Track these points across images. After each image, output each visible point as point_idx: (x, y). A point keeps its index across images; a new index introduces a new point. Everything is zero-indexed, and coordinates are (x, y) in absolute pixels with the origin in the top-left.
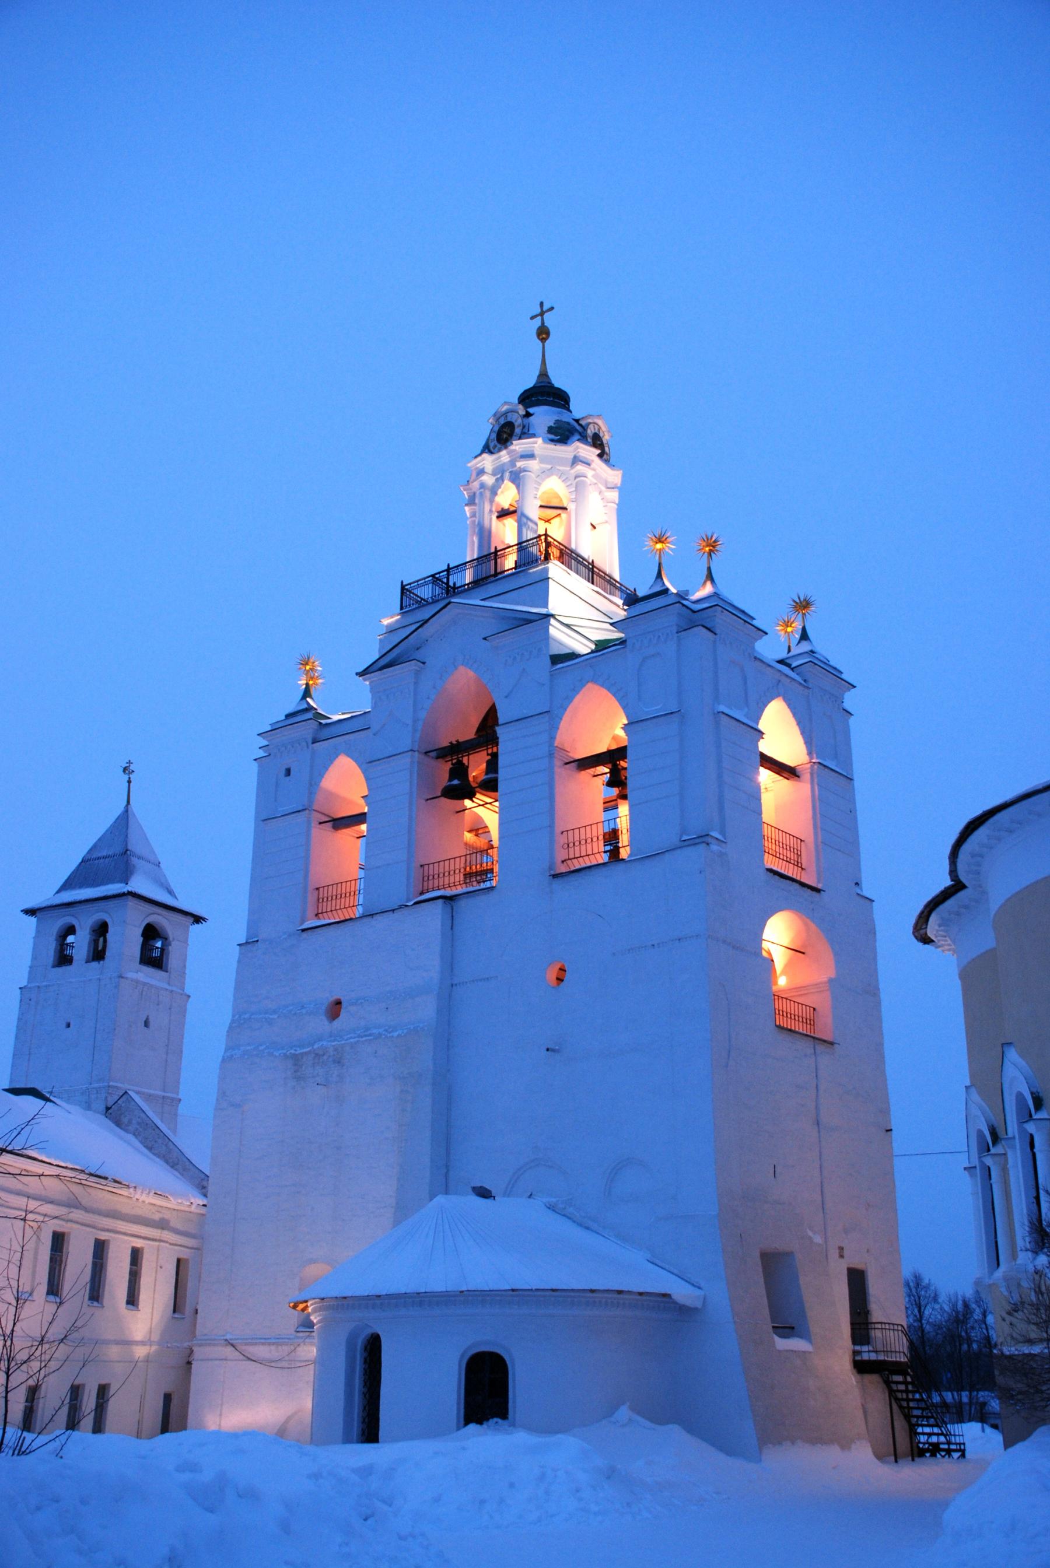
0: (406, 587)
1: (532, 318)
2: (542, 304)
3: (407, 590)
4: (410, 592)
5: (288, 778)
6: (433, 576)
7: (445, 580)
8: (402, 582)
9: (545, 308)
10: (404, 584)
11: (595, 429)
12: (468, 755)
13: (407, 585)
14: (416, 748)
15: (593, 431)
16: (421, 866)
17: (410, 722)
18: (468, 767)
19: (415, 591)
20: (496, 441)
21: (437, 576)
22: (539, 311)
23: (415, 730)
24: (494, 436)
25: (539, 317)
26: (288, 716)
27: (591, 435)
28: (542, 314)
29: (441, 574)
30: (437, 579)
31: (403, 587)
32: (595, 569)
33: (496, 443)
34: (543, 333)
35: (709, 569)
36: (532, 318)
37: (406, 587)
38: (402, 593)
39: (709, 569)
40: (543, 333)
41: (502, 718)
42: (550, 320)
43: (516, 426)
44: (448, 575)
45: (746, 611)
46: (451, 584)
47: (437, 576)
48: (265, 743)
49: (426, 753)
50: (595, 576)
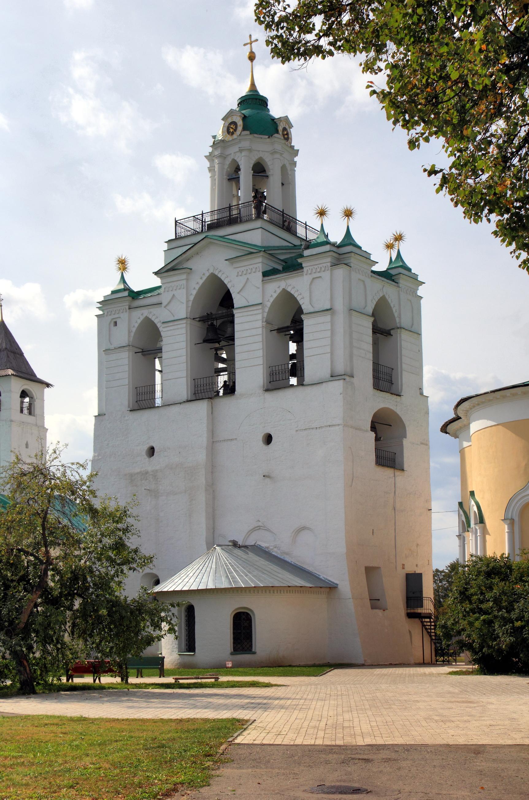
1: (245, 45)
5: (116, 327)
6: (194, 217)
9: (253, 39)
12: (217, 320)
14: (188, 317)
17: (185, 301)
20: (226, 133)
21: (196, 217)
23: (187, 307)
25: (249, 45)
26: (113, 292)
28: (251, 44)
30: (197, 218)
31: (176, 222)
32: (284, 215)
36: (245, 45)
38: (176, 225)
41: (236, 303)
44: (202, 216)
46: (204, 221)
49: (194, 319)
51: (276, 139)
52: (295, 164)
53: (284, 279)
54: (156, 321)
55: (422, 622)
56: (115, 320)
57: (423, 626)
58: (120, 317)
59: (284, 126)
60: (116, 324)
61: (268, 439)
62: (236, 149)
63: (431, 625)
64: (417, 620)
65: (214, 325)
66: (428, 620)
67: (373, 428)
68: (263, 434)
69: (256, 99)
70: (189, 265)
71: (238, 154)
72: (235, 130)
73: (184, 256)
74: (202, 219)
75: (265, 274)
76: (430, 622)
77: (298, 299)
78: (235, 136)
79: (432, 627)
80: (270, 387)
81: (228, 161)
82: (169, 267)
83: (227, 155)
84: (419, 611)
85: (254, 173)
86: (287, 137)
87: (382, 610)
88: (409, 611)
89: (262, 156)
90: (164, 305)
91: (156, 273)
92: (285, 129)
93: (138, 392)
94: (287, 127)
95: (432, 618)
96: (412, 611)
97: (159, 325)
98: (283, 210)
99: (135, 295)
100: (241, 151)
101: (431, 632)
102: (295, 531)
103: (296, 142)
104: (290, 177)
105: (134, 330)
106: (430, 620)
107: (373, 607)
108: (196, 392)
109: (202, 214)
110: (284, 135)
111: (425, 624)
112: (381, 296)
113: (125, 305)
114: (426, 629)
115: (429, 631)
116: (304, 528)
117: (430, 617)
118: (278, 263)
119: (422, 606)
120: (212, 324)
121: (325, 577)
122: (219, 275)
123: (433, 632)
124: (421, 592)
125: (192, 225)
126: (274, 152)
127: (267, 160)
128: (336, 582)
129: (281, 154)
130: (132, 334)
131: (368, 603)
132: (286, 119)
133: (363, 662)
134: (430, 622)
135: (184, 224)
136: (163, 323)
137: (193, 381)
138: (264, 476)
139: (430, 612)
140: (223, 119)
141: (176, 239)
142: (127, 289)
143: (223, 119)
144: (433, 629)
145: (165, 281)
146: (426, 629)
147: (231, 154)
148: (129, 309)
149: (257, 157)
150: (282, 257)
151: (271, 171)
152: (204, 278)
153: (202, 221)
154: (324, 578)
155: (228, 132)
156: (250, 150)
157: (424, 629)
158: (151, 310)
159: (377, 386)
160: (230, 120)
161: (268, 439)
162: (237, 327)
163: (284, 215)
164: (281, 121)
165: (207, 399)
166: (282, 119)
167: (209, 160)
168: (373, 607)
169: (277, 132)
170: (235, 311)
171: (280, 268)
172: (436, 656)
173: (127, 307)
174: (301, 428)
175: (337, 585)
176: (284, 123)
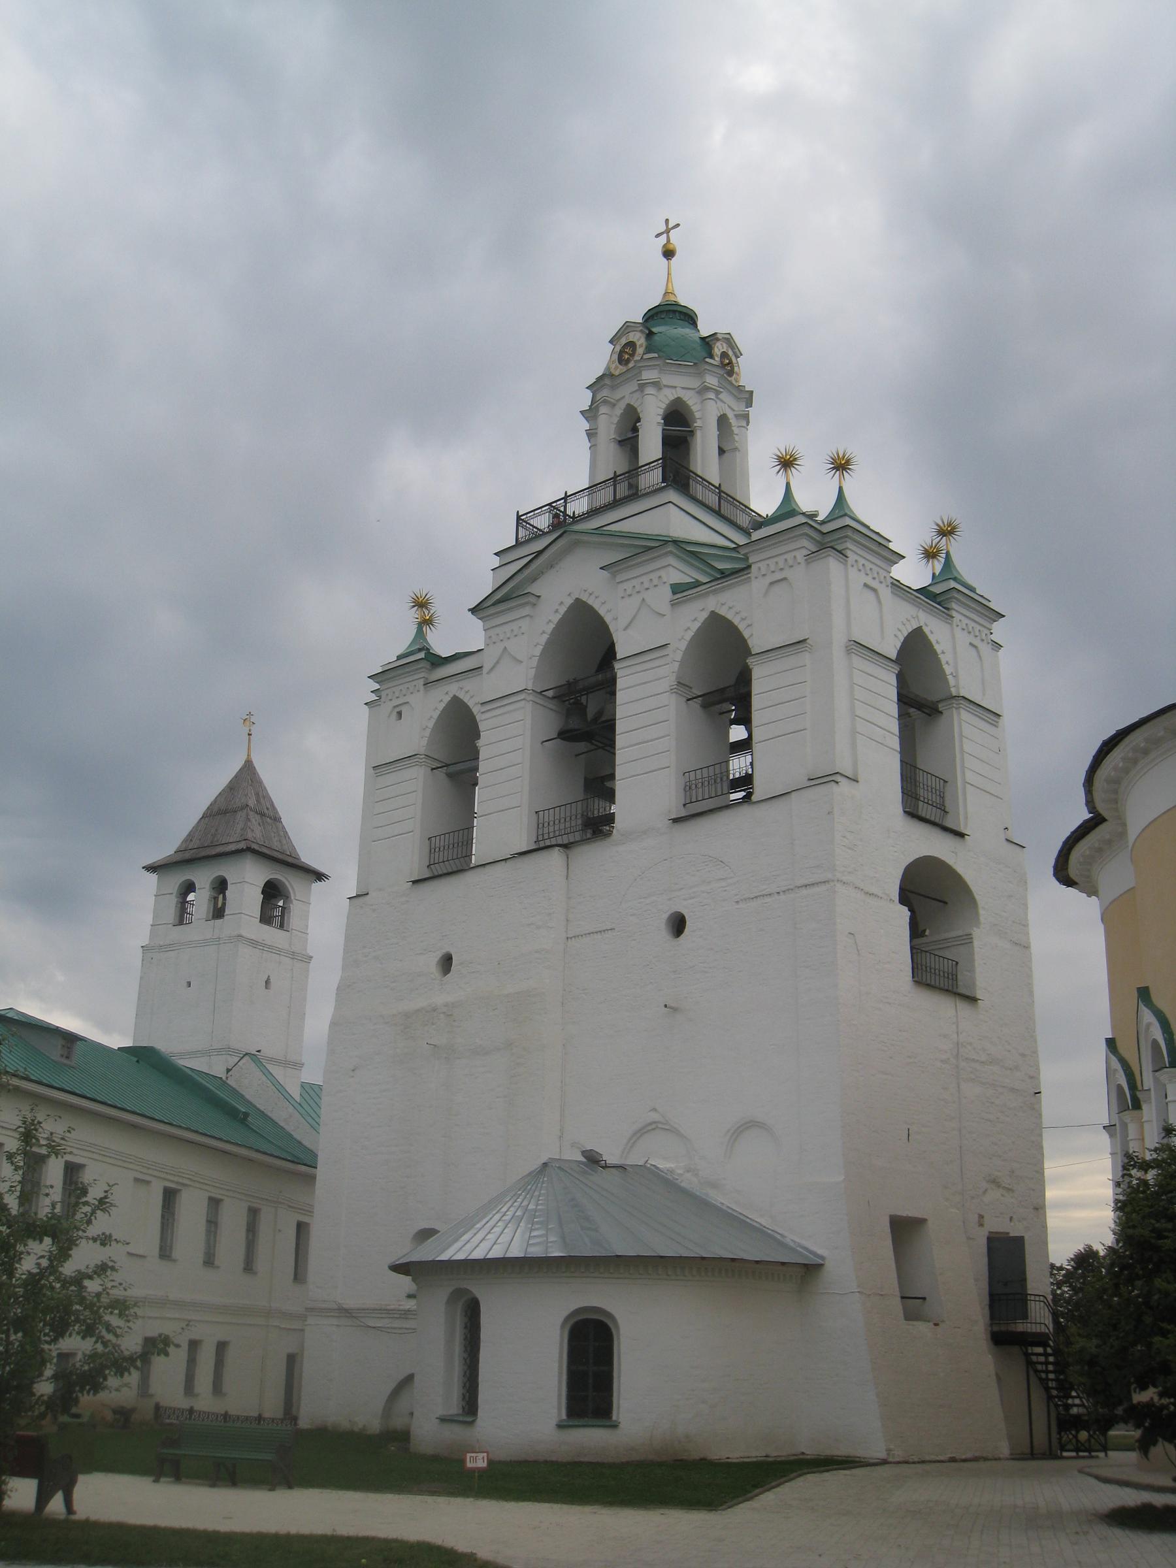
0: (522, 518)
1: (658, 236)
2: (667, 221)
6: (550, 504)
7: (562, 509)
8: (518, 512)
9: (670, 226)
11: (723, 348)
16: (536, 812)
18: (586, 707)
19: (531, 522)
21: (554, 505)
22: (663, 228)
24: (616, 357)
26: (399, 658)
27: (719, 353)
28: (667, 231)
29: (558, 503)
31: (519, 517)
33: (618, 364)
34: (669, 253)
35: (841, 489)
36: (658, 236)
37: (522, 518)
39: (841, 489)
40: (669, 253)
43: (638, 346)
44: (566, 502)
45: (881, 533)
47: (554, 505)
48: (377, 686)
50: (722, 501)
51: (707, 367)
52: (746, 417)
53: (715, 592)
54: (471, 704)
55: (1027, 1355)
56: (398, 709)
57: (1030, 1364)
58: (408, 703)
59: (725, 350)
61: (678, 925)
62: (633, 386)
63: (1047, 1363)
64: (1016, 1349)
65: (582, 704)
66: (1040, 1350)
68: (666, 916)
69: (674, 312)
70: (535, 588)
72: (633, 355)
73: (527, 572)
76: (1046, 1355)
77: (741, 627)
78: (631, 365)
79: (1051, 1368)
80: (683, 813)
81: (619, 411)
83: (618, 400)
84: (1020, 1327)
86: (728, 366)
87: (931, 1324)
88: (996, 1329)
89: (682, 397)
90: (485, 670)
91: (473, 611)
92: (724, 355)
94: (730, 353)
95: (1049, 1346)
96: (1003, 1328)
97: (475, 710)
98: (720, 484)
99: (436, 661)
101: (1048, 1379)
102: (732, 1132)
103: (747, 373)
104: (737, 438)
106: (1045, 1350)
107: (911, 1316)
108: (540, 838)
111: (1034, 1358)
114: (1036, 1371)
115: (1043, 1375)
116: (749, 1125)
117: (1044, 1345)
119: (1025, 1316)
120: (577, 703)
121: (797, 1240)
122: (590, 602)
123: (1052, 1380)
124: (1023, 1280)
126: (703, 390)
127: (690, 403)
128: (820, 1252)
129: (717, 393)
131: (896, 1304)
132: (729, 340)
133: (882, 1455)
134: (1046, 1355)
138: (666, 1006)
139: (1043, 1329)
140: (611, 342)
142: (426, 649)
143: (611, 342)
144: (1051, 1372)
145: (490, 624)
146: (1036, 1371)
147: (624, 397)
152: (563, 610)
154: (794, 1242)
155: (621, 360)
156: (657, 385)
157: (1031, 1373)
159: (912, 813)
160: (623, 341)
161: (678, 925)
162: (620, 697)
163: (722, 494)
164: (718, 340)
165: (558, 848)
167: (586, 419)
168: (911, 1316)
169: (711, 356)
170: (617, 666)
172: (1059, 1433)
173: (422, 682)
175: (822, 1258)
176: (725, 345)
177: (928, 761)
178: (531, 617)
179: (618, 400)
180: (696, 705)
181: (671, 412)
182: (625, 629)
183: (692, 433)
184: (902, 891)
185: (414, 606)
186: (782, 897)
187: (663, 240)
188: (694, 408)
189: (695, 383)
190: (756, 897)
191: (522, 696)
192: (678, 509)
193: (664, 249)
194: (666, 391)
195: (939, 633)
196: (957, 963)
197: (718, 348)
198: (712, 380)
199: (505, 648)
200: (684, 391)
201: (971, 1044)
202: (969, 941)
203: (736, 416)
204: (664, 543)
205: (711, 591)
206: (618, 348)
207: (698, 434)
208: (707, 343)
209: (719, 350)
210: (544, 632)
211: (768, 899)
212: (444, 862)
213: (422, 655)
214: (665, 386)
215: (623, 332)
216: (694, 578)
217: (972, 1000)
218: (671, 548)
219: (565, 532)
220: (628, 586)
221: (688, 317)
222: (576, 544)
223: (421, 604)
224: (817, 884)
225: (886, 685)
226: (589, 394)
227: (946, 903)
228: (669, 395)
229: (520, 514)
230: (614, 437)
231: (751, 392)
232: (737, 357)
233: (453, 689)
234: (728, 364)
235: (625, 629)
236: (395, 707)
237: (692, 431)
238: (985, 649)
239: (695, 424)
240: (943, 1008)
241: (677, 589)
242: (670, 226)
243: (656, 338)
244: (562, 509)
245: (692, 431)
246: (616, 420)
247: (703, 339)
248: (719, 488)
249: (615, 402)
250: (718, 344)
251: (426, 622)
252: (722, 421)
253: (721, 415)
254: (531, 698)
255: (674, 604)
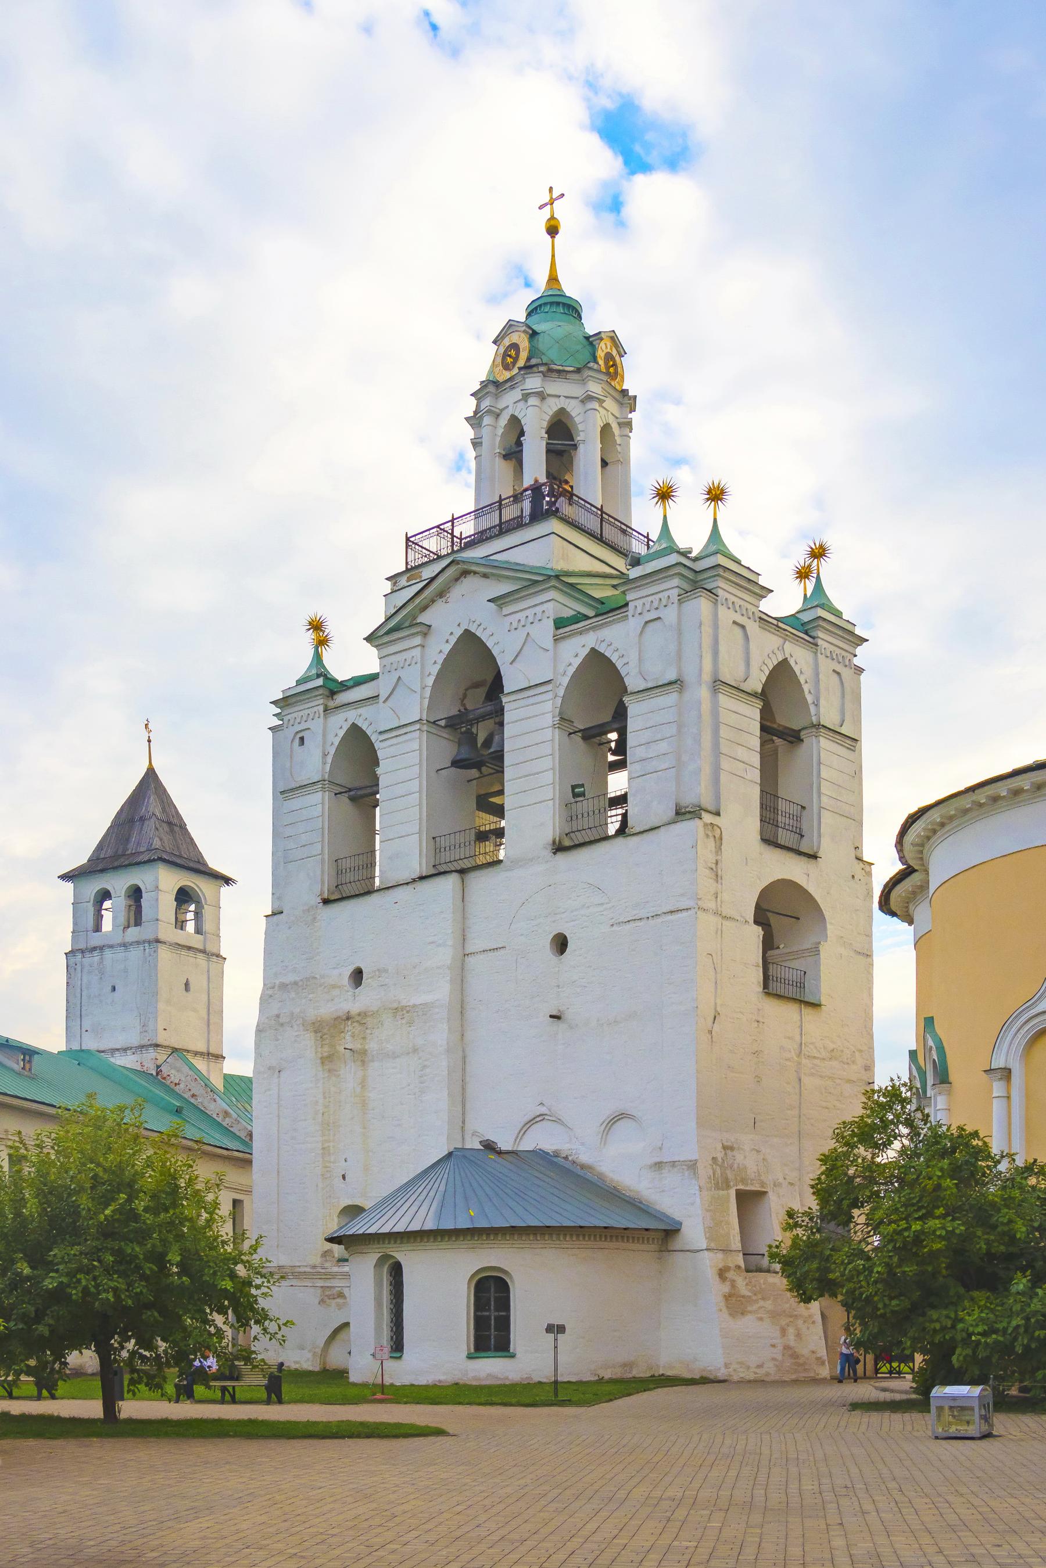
0: (412, 539)
1: (541, 207)
3: (413, 543)
4: (416, 544)
6: (438, 527)
7: (450, 531)
10: (408, 536)
11: (607, 347)
12: (477, 723)
13: (411, 537)
15: (605, 351)
17: (418, 689)
18: (477, 735)
21: (442, 527)
22: (547, 199)
23: (422, 698)
24: (499, 360)
28: (552, 204)
30: (443, 530)
31: (408, 539)
34: (553, 230)
36: (541, 207)
37: (412, 539)
38: (407, 546)
40: (553, 230)
42: (561, 210)
44: (453, 525)
46: (457, 533)
47: (442, 527)
50: (604, 523)
51: (591, 373)
54: (369, 732)
56: (300, 735)
58: (309, 729)
59: (609, 350)
60: (302, 739)
61: (561, 944)
62: (516, 394)
67: (761, 917)
69: (558, 304)
71: (521, 404)
74: (453, 530)
75: (560, 623)
81: (504, 421)
82: (392, 624)
83: (502, 410)
85: (549, 438)
86: (613, 370)
90: (382, 699)
91: (369, 639)
92: (609, 357)
93: (340, 867)
94: (614, 353)
97: (373, 738)
100: (526, 397)
105: (332, 751)
109: (453, 521)
110: (608, 368)
112: (780, 659)
113: (318, 705)
118: (586, 603)
125: (433, 544)
127: (573, 414)
130: (329, 759)
132: (614, 339)
135: (420, 544)
136: (380, 733)
137: (432, 842)
140: (495, 342)
141: (407, 570)
142: (324, 674)
143: (495, 342)
147: (508, 407)
148: (325, 710)
149: (555, 409)
150: (597, 594)
151: (581, 434)
152: (453, 640)
153: (452, 534)
156: (542, 396)
158: (360, 711)
161: (561, 944)
163: (604, 515)
166: (603, 335)
169: (595, 361)
170: (505, 700)
171: (591, 613)
173: (321, 708)
174: (620, 920)
177: (789, 789)
178: (424, 646)
179: (502, 410)
180: (577, 738)
181: (551, 425)
182: (511, 663)
183: (575, 447)
184: (758, 908)
185: (309, 629)
186: (651, 921)
187: (546, 213)
188: (577, 420)
189: (577, 391)
190: (629, 921)
191: (417, 726)
192: (561, 539)
193: (548, 225)
194: (551, 401)
195: (800, 659)
196: (805, 973)
197: (603, 349)
198: (595, 388)
199: (400, 677)
200: (568, 400)
201: (812, 1043)
202: (817, 953)
203: (619, 424)
204: (545, 578)
205: (590, 628)
206: (502, 350)
207: (581, 448)
208: (591, 341)
209: (603, 351)
210: (435, 663)
211: (638, 923)
212: (350, 882)
213: (320, 682)
214: (549, 395)
215: (506, 332)
216: (576, 611)
217: (816, 1006)
218: (553, 583)
219: (452, 562)
220: (514, 618)
221: (572, 310)
222: (465, 573)
223: (316, 626)
224: (681, 910)
225: (751, 714)
226: (473, 402)
227: (798, 919)
228: (552, 406)
229: (408, 536)
230: (498, 451)
231: (635, 397)
232: (621, 356)
233: (351, 716)
234: (612, 366)
235: (511, 663)
236: (297, 732)
237: (575, 445)
238: (846, 673)
239: (579, 438)
240: (789, 1012)
241: (560, 623)
242: (554, 197)
243: (540, 338)
244: (450, 531)
245: (575, 445)
246: (500, 431)
247: (587, 338)
248: (601, 510)
249: (498, 411)
250: (602, 344)
251: (322, 642)
252: (606, 429)
253: (604, 425)
254: (425, 728)
255: (557, 640)
